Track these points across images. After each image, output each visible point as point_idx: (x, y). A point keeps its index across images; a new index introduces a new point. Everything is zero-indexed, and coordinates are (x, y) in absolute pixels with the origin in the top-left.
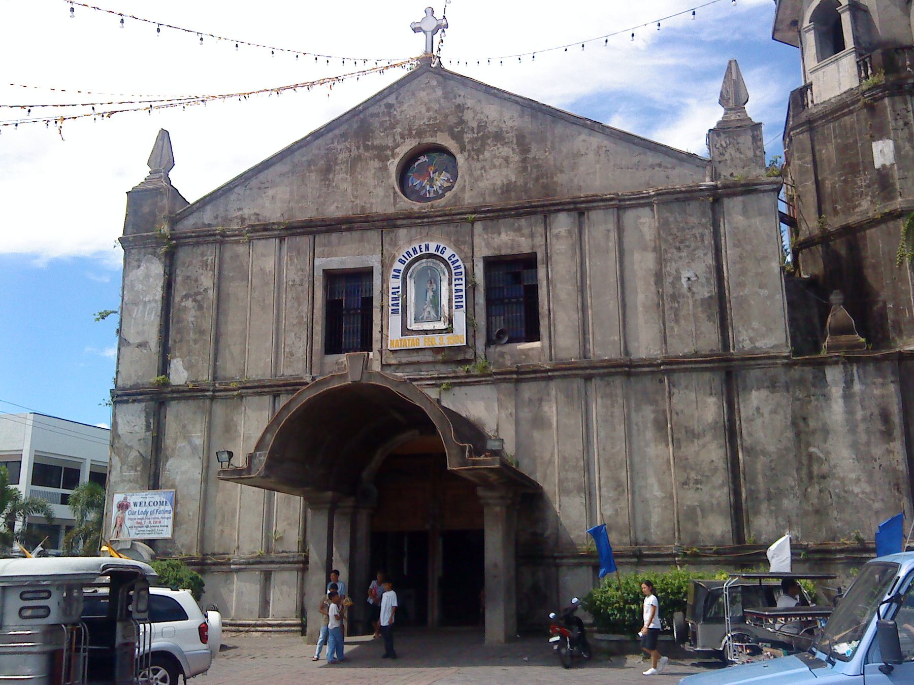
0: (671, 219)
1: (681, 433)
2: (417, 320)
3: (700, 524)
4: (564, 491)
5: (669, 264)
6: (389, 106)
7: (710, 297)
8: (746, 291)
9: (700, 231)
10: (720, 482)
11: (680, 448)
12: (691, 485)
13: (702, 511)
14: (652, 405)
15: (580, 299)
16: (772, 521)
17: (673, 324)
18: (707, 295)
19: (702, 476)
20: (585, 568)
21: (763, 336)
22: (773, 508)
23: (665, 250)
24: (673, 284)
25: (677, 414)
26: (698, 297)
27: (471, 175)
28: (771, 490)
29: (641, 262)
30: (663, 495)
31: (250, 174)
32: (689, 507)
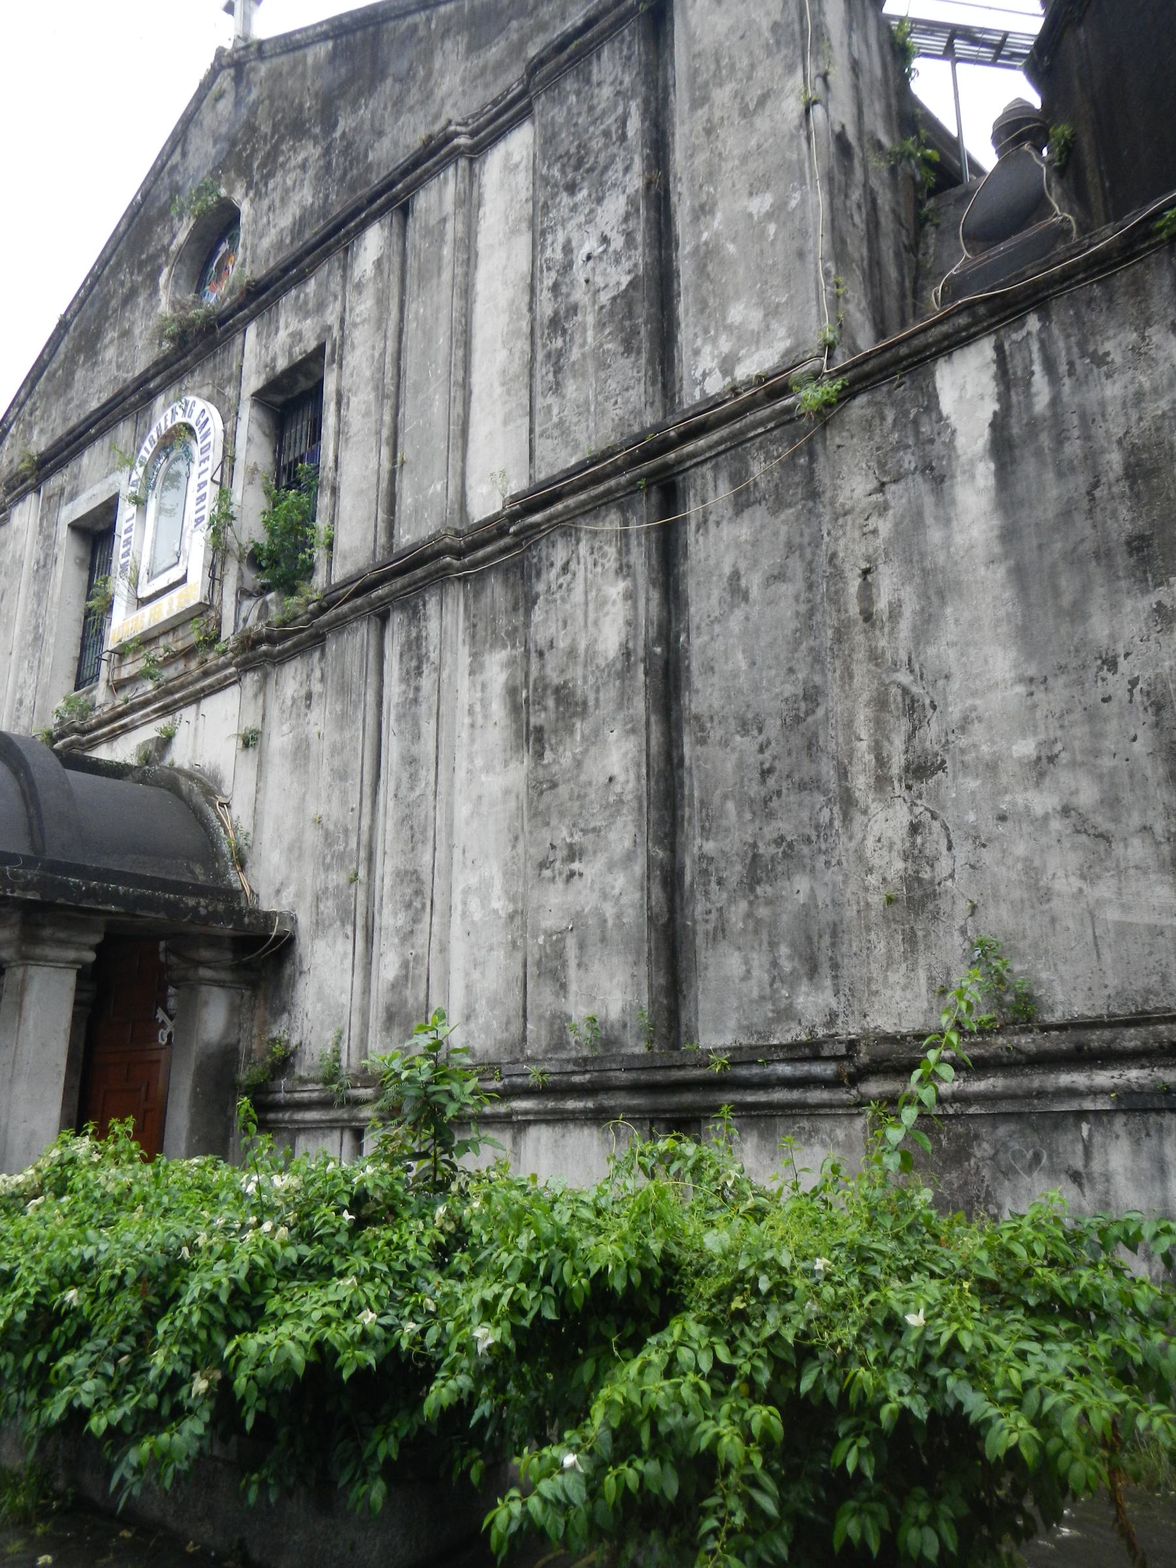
0: (560, 119)
1: (545, 709)
2: (152, 575)
3: (573, 987)
4: (320, 925)
5: (550, 238)
6: (174, 168)
7: (631, 283)
8: (717, 222)
9: (620, 110)
10: (627, 843)
11: (540, 755)
12: (558, 864)
13: (582, 946)
14: (504, 646)
15: (387, 418)
16: (759, 960)
17: (551, 399)
18: (625, 280)
19: (585, 832)
20: (336, 1135)
21: (757, 339)
22: (762, 912)
23: (545, 205)
24: (555, 288)
25: (541, 654)
26: (604, 298)
27: (253, 233)
28: (762, 849)
29: (505, 268)
30: (511, 908)
31: (23, 394)
32: (548, 934)
